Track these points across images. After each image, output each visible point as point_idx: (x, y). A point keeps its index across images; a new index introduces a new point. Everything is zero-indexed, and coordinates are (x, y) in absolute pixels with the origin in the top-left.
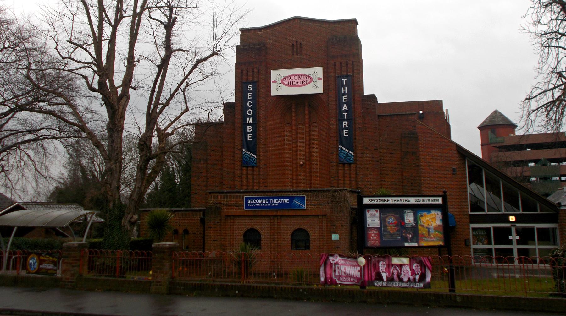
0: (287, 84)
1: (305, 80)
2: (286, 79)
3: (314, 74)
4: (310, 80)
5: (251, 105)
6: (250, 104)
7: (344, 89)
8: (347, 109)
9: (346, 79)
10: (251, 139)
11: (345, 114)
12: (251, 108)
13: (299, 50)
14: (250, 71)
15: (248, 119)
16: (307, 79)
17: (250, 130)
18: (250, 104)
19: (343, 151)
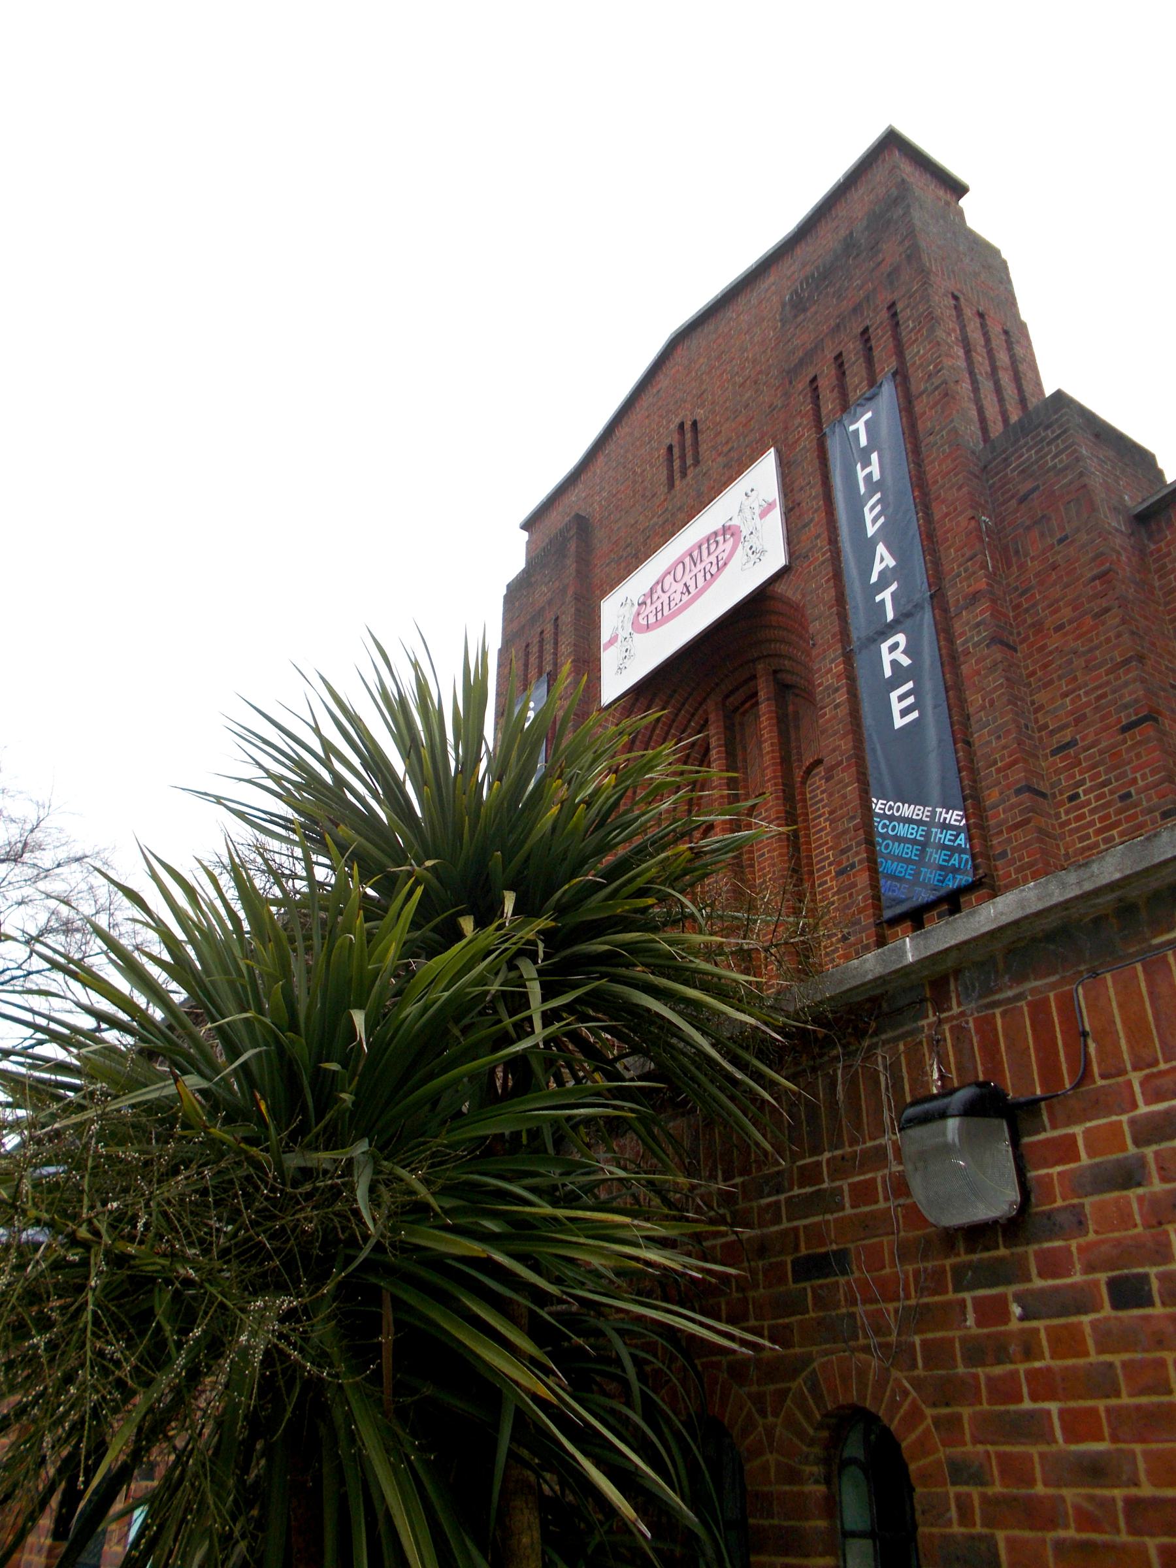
3: (747, 503)
4: (731, 542)
7: (867, 463)
9: (869, 415)
11: (886, 596)
14: (534, 649)
16: (721, 548)
19: (903, 830)
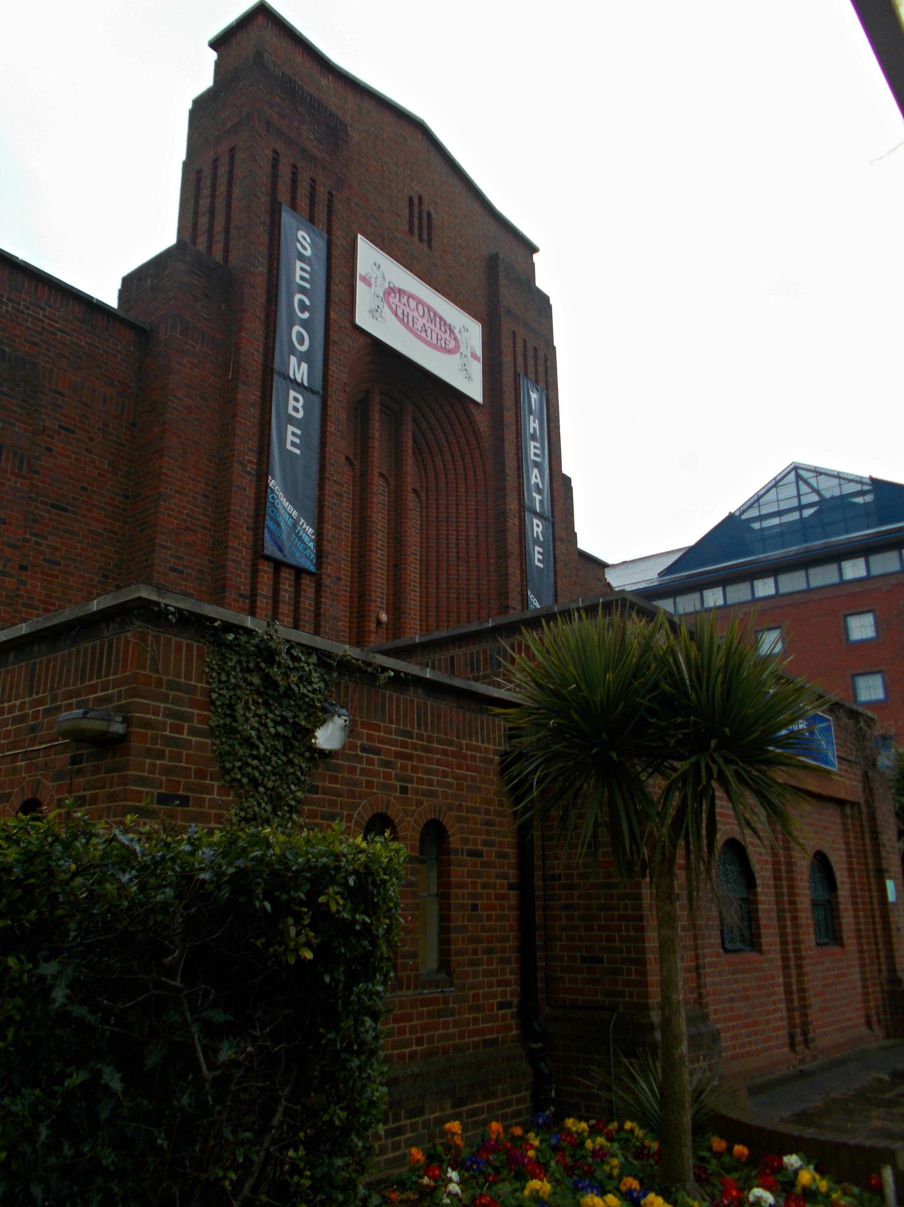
0: (399, 312)
1: (444, 336)
2: (397, 295)
5: (306, 315)
6: (303, 307)
8: (541, 486)
10: (298, 452)
12: (305, 324)
13: (425, 231)
15: (293, 360)
17: (296, 410)
18: (303, 307)
